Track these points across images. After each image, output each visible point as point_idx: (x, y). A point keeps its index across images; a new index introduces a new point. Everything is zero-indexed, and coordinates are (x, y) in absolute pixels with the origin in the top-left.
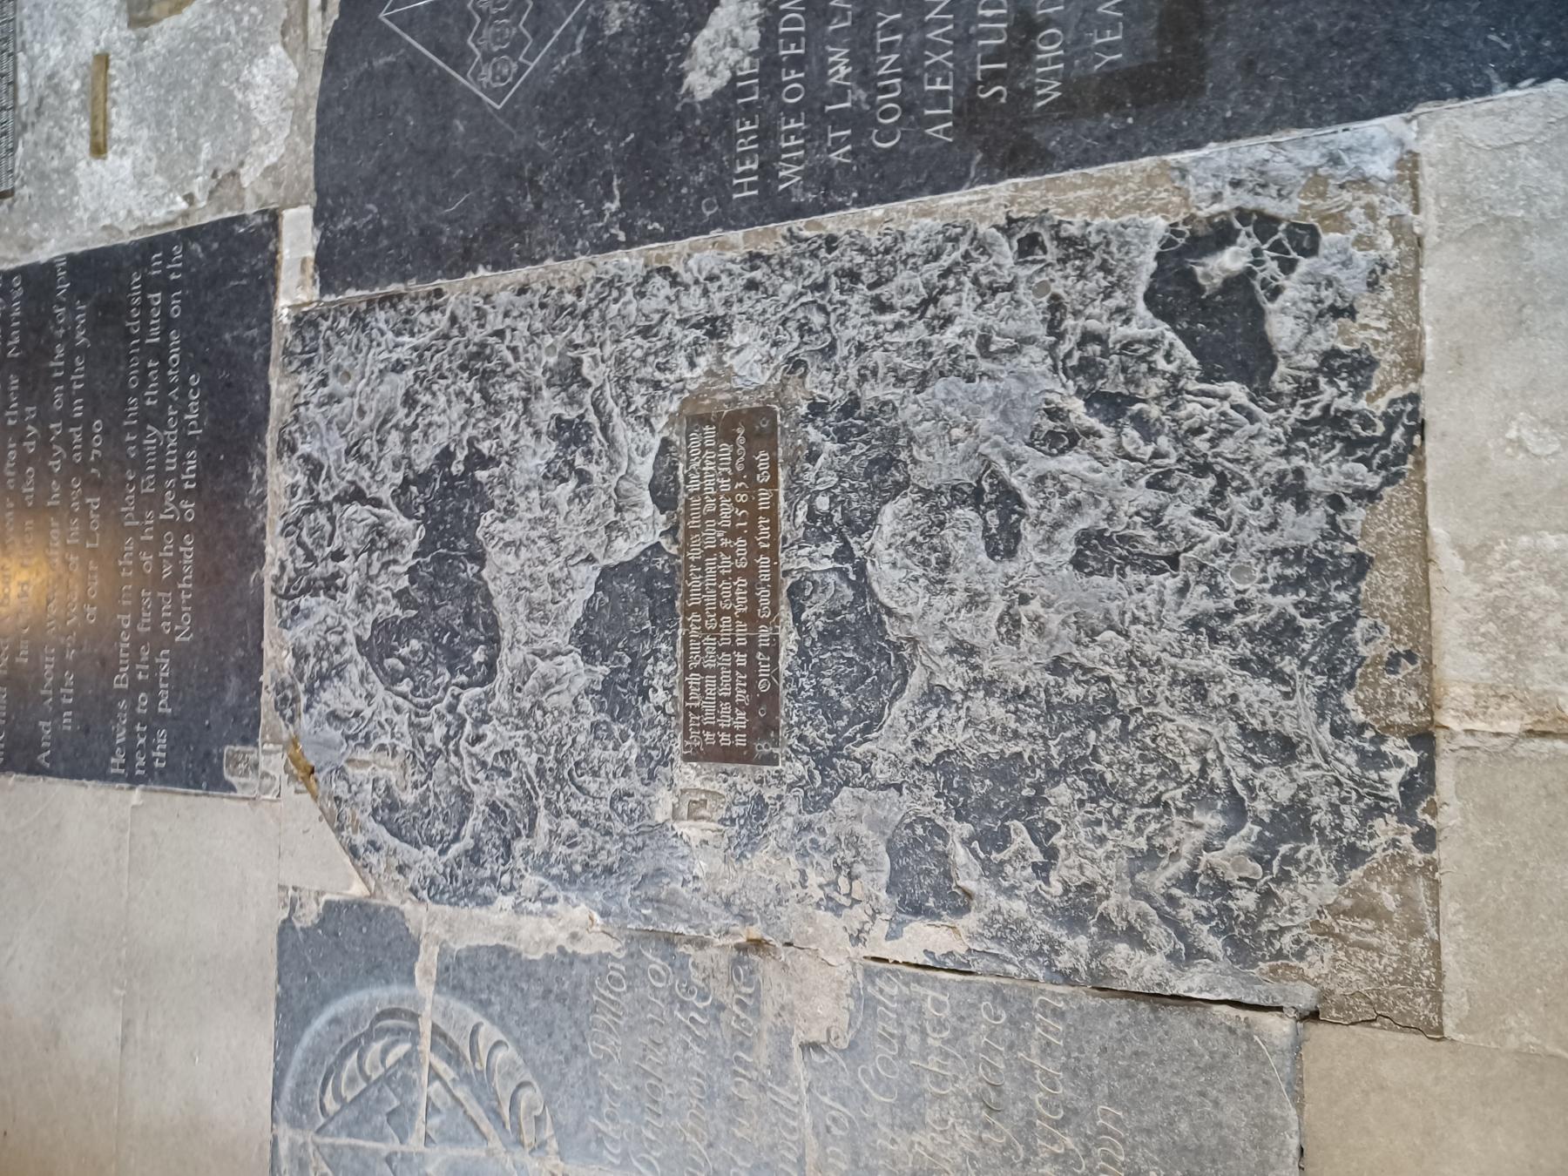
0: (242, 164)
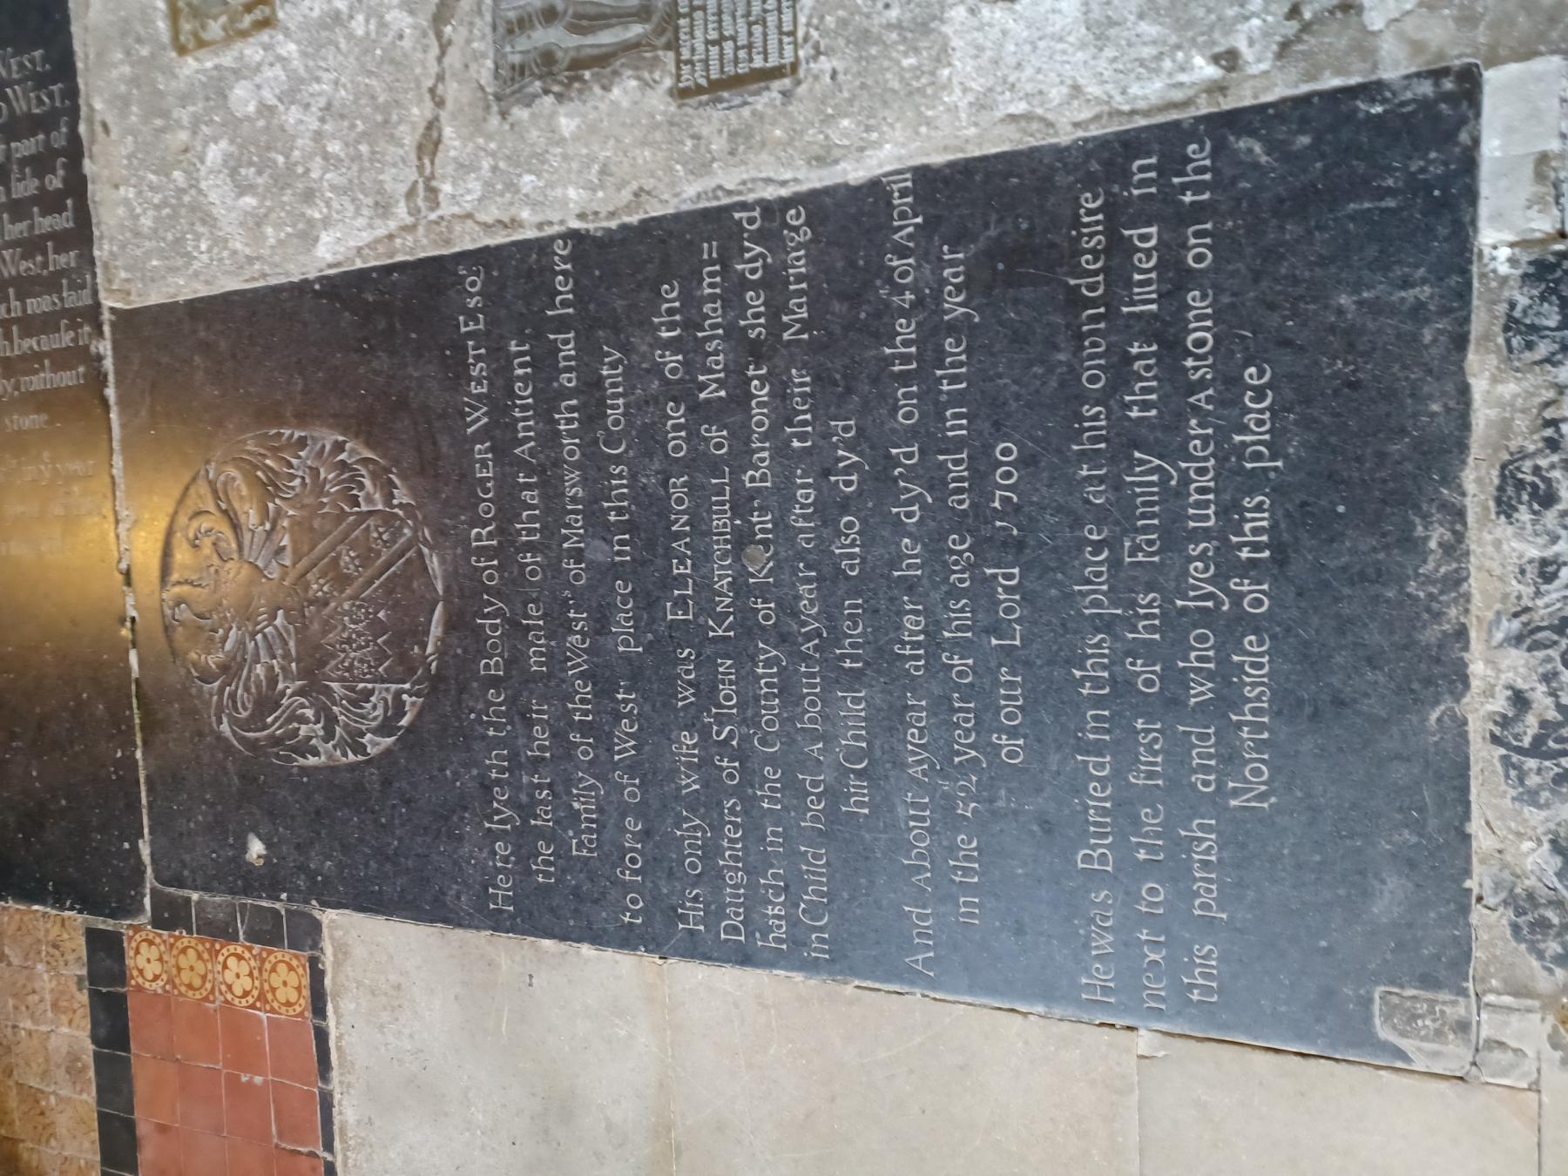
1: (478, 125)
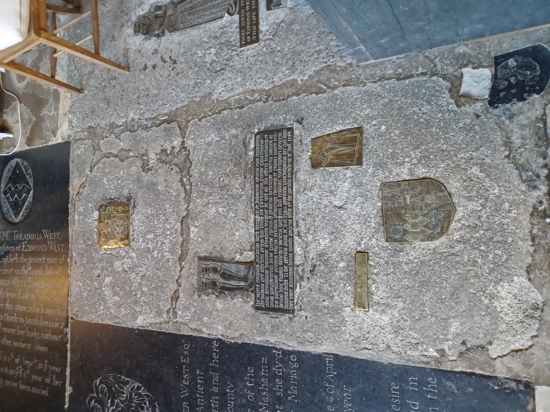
0: (490, 343)
1: (191, 297)
